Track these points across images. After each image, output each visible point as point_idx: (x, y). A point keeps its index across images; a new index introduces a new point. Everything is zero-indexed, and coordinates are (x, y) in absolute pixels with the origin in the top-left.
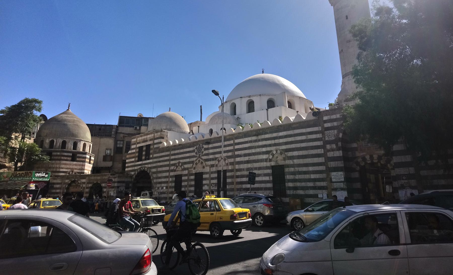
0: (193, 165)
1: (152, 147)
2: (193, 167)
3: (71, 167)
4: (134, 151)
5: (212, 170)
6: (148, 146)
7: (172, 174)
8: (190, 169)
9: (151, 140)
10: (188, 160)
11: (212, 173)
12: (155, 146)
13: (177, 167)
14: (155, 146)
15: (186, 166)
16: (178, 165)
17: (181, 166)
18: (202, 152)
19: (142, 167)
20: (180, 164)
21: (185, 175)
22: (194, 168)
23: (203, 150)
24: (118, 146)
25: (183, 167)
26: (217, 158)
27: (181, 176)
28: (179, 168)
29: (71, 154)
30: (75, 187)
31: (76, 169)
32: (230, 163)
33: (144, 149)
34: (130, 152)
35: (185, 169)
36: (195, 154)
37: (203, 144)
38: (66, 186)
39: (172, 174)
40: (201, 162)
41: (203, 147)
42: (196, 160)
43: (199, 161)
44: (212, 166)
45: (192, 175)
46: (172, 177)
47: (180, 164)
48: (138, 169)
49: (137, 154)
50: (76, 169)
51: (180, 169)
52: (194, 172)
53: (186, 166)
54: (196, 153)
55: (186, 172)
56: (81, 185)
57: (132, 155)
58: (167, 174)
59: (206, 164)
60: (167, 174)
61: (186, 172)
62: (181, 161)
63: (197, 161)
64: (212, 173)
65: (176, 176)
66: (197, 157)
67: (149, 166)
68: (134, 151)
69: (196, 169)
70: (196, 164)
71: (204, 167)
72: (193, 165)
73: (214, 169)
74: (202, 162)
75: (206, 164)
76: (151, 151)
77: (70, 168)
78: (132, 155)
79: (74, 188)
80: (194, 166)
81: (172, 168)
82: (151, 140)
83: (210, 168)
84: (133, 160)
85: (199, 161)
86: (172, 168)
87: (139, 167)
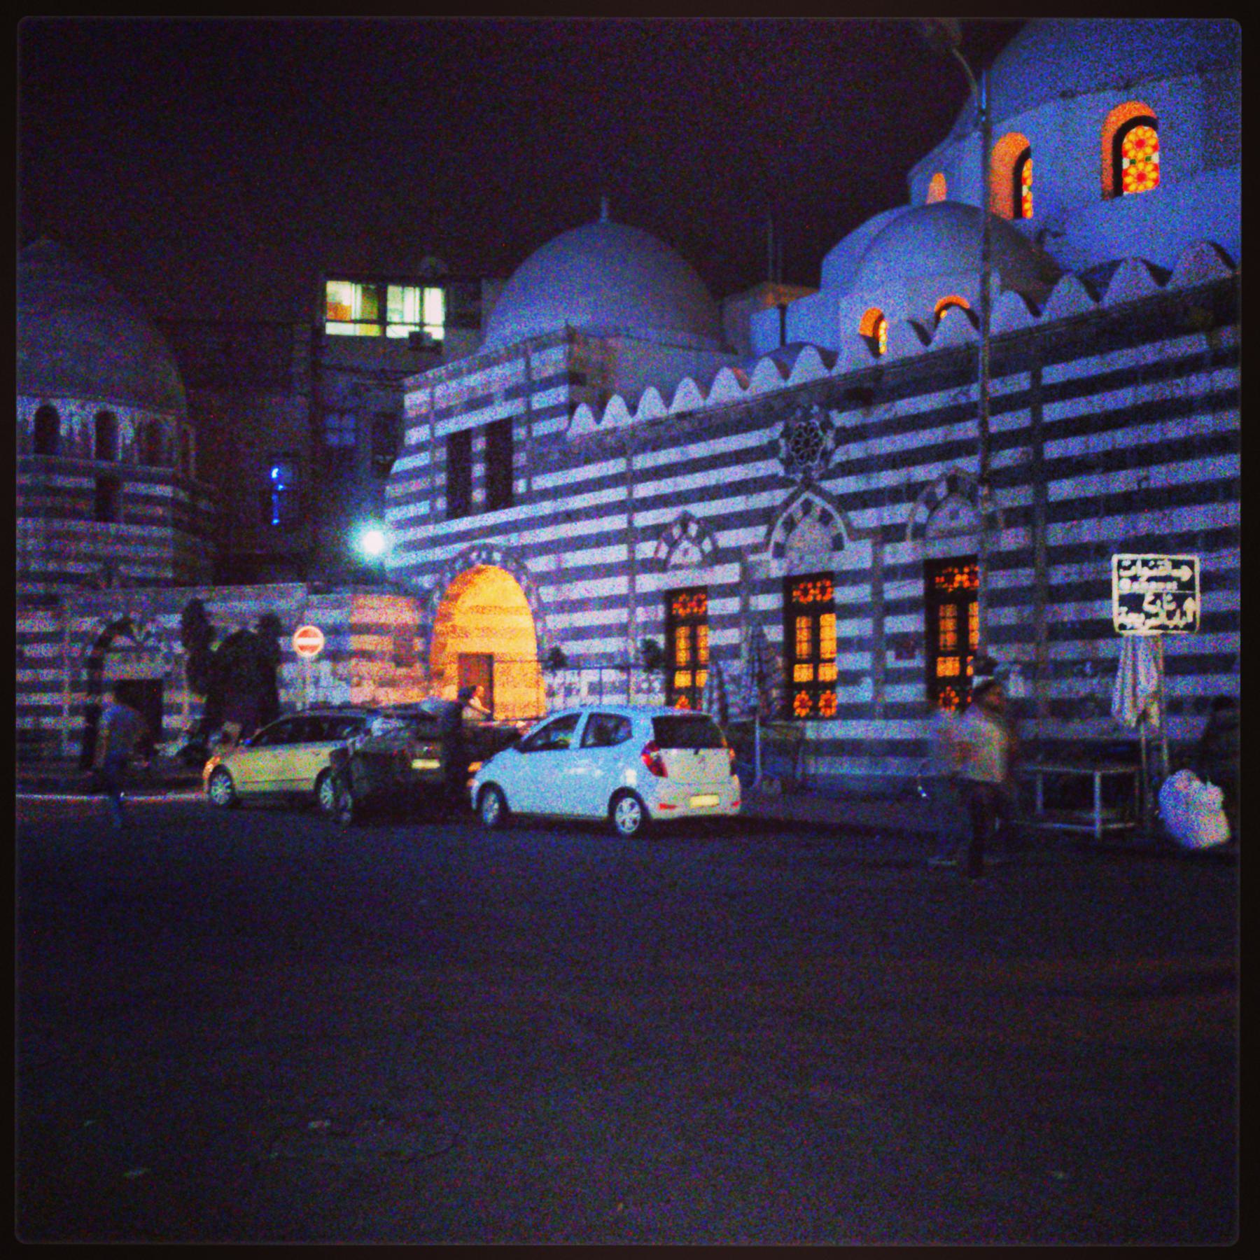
0: (769, 534)
1: (519, 433)
2: (772, 543)
3: (101, 549)
4: (422, 460)
5: (889, 561)
6: (499, 432)
7: (649, 583)
8: (753, 558)
9: (511, 393)
10: (737, 504)
11: (892, 573)
12: (543, 428)
13: (673, 545)
14: (543, 428)
15: (728, 539)
16: (676, 532)
17: (698, 540)
18: (827, 455)
19: (472, 549)
20: (693, 529)
21: (726, 591)
22: (780, 551)
23: (829, 442)
24: (333, 440)
25: (707, 546)
26: (923, 485)
27: (699, 593)
28: (686, 552)
29: (88, 483)
30: (133, 655)
31: (127, 560)
32: (1010, 512)
33: (479, 445)
34: (400, 465)
35: (719, 557)
36: (780, 470)
37: (828, 405)
38: (83, 650)
39: (649, 583)
40: (816, 513)
41: (827, 425)
42: (787, 503)
43: (807, 506)
44: (890, 534)
45: (767, 586)
46: (647, 599)
47: (693, 529)
48: (454, 560)
49: (441, 479)
50: (127, 560)
51: (695, 555)
52: (776, 569)
53: (728, 539)
54: (787, 463)
55: (728, 573)
56: (163, 646)
57: (414, 486)
58: (618, 585)
59: (849, 525)
60: (618, 585)
61: (728, 573)
62: (700, 510)
63: (796, 506)
64: (892, 573)
65: (669, 597)
66: (793, 482)
67: (514, 539)
68: (422, 460)
69: (793, 555)
70: (790, 525)
71: (837, 544)
72: (769, 534)
73: (902, 553)
74: (824, 511)
75: (849, 525)
76: (520, 459)
77: (93, 558)
78: (414, 486)
79: (125, 661)
80: (778, 535)
81: (647, 549)
82: (511, 393)
83: (875, 544)
84: (423, 508)
85: (807, 506)
86: (647, 549)
87: (460, 546)
